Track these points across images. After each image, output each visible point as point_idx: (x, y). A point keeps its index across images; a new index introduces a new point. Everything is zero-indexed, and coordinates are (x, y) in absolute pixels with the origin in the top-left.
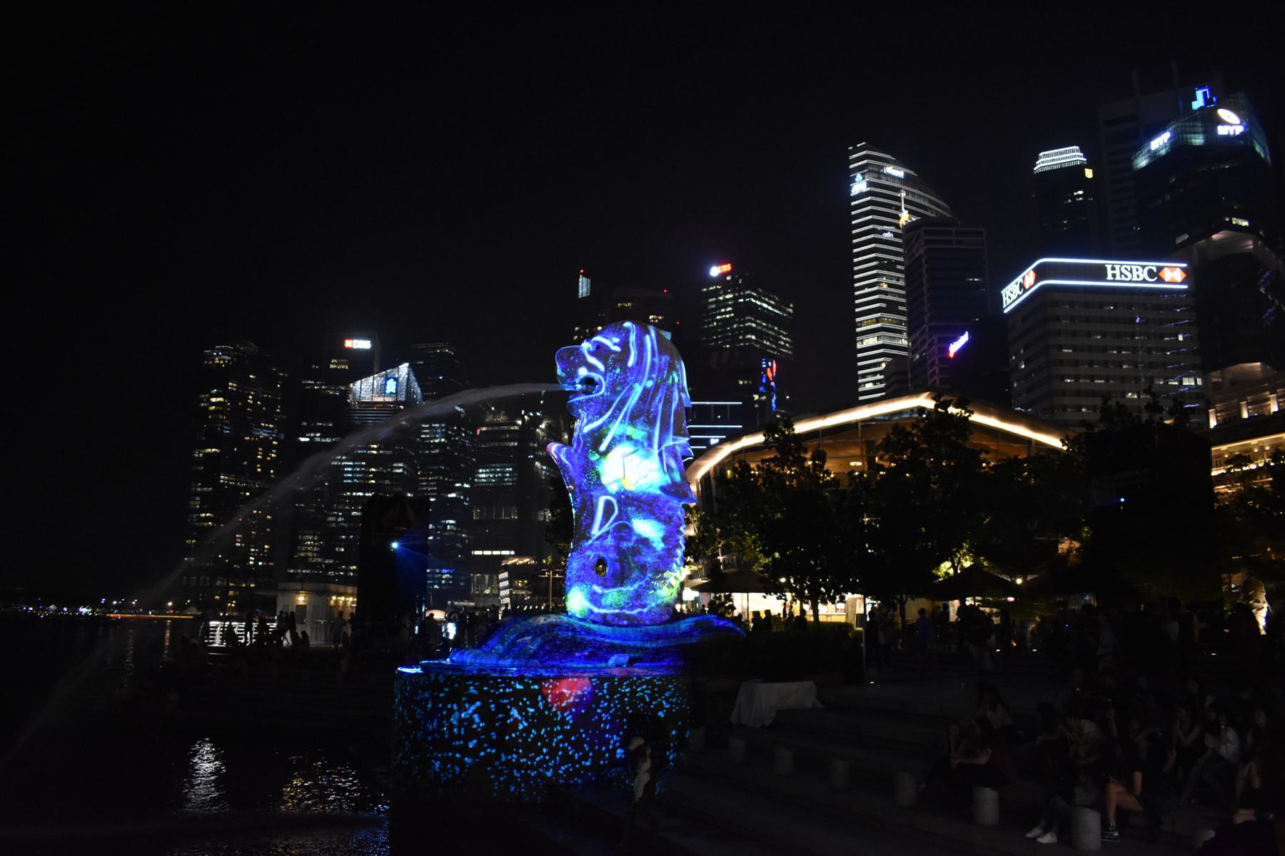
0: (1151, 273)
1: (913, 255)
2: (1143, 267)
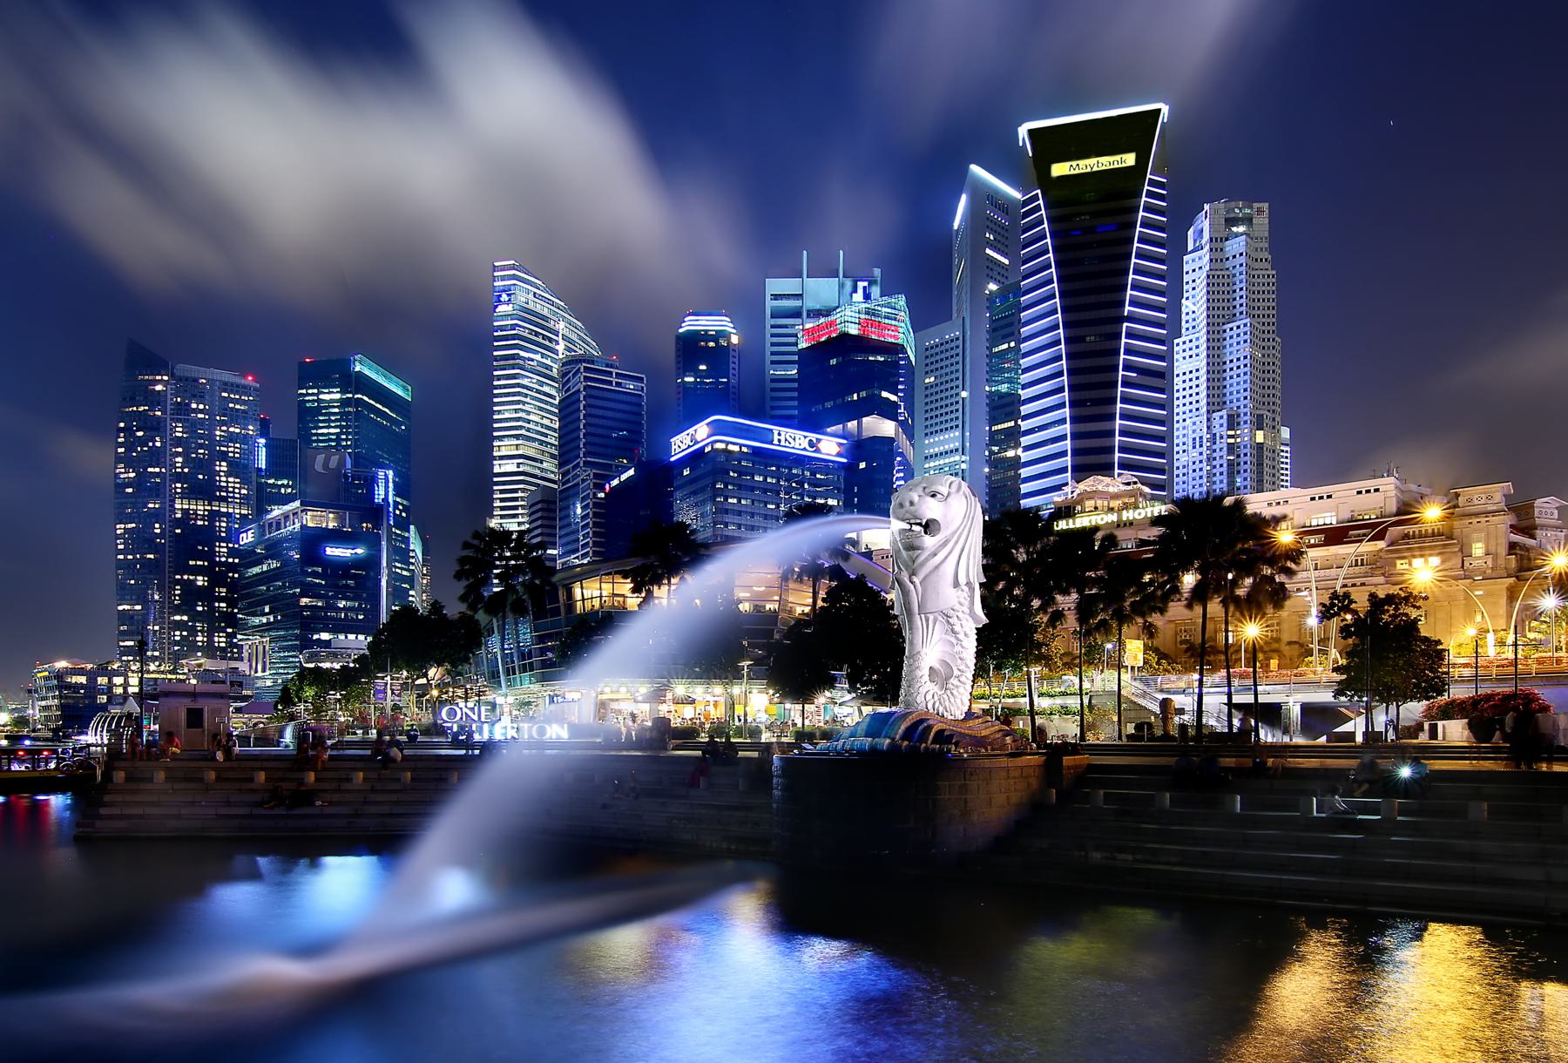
0: (811, 444)
1: (568, 390)
2: (805, 437)
